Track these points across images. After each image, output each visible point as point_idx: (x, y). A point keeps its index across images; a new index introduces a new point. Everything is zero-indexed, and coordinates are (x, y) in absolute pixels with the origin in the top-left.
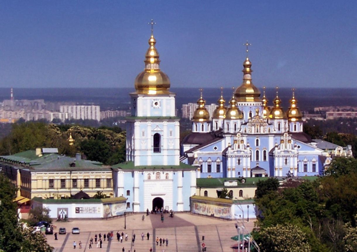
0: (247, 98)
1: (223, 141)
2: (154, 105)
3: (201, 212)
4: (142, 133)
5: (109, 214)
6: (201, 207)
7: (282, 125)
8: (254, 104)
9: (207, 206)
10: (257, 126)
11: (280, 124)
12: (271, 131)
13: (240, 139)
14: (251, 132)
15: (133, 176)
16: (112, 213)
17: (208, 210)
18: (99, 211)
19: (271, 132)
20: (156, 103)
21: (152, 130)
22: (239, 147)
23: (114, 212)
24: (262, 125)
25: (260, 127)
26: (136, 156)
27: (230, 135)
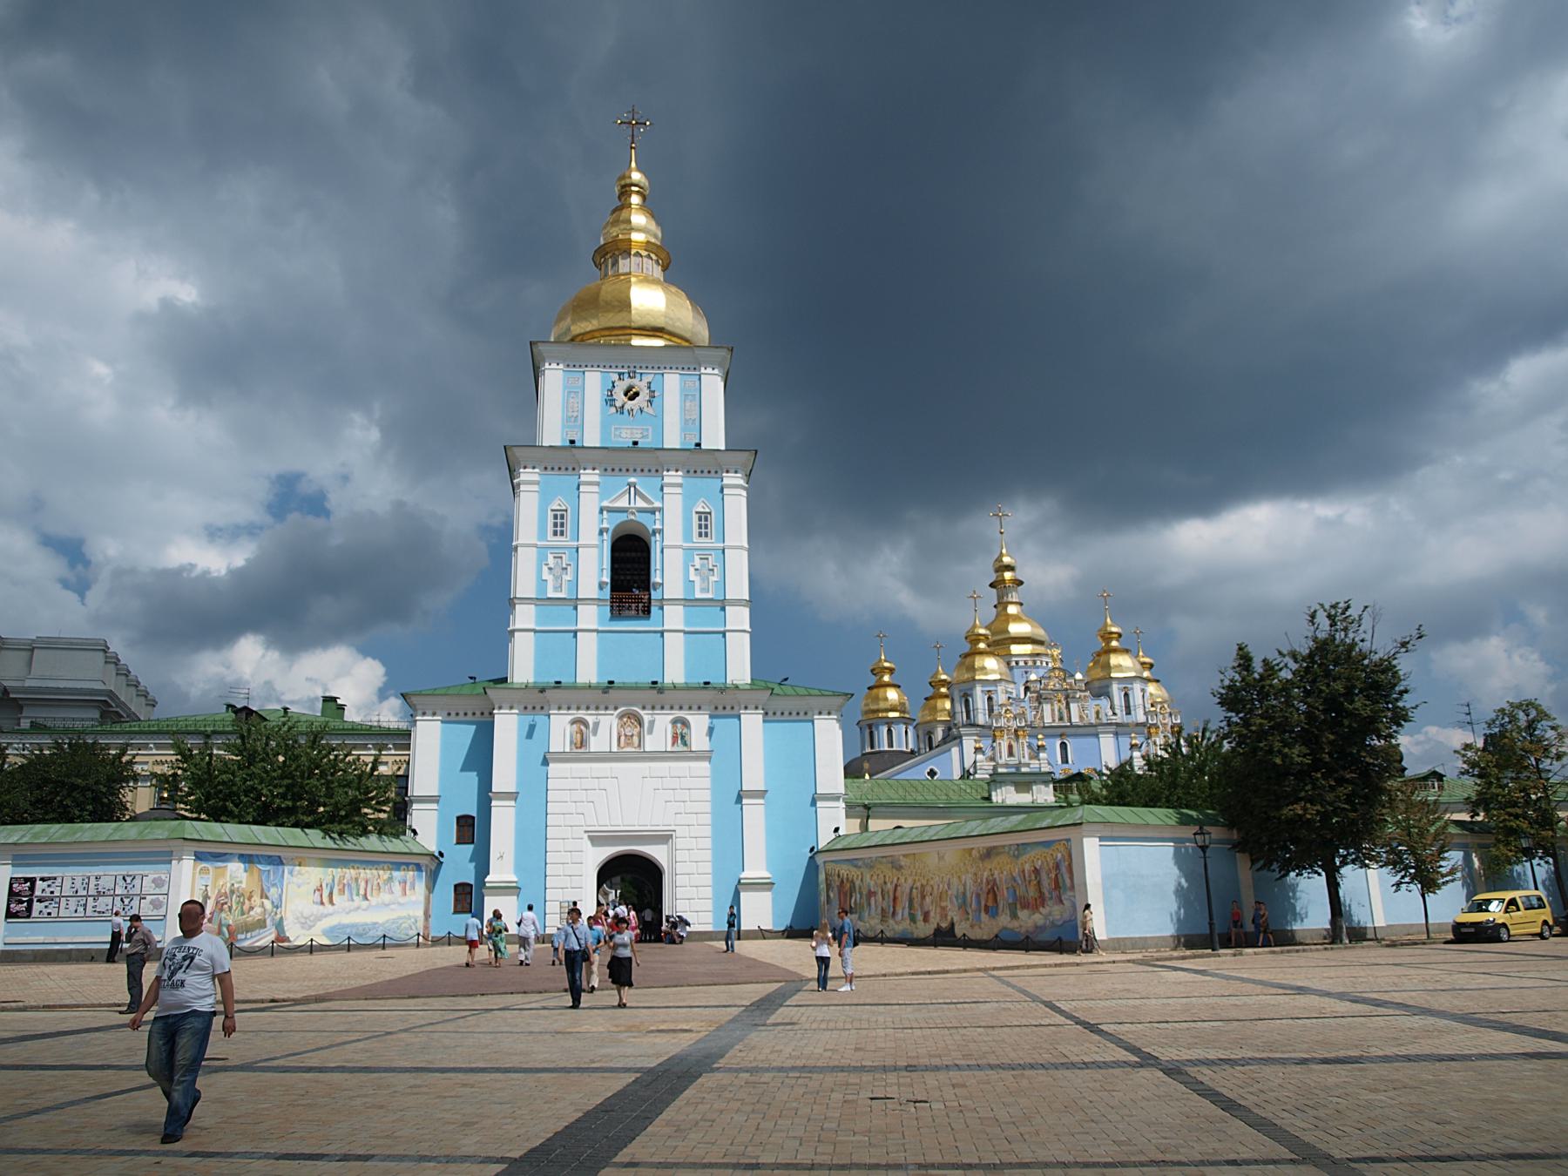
1: (955, 751)
3: (871, 923)
5: (261, 924)
6: (871, 894)
10: (1059, 701)
11: (1130, 692)
13: (1014, 724)
14: (1042, 717)
16: (279, 925)
17: (911, 906)
18: (156, 905)
19: (1105, 721)
20: (632, 395)
21: (605, 504)
22: (1011, 754)
23: (306, 924)
25: (1068, 704)
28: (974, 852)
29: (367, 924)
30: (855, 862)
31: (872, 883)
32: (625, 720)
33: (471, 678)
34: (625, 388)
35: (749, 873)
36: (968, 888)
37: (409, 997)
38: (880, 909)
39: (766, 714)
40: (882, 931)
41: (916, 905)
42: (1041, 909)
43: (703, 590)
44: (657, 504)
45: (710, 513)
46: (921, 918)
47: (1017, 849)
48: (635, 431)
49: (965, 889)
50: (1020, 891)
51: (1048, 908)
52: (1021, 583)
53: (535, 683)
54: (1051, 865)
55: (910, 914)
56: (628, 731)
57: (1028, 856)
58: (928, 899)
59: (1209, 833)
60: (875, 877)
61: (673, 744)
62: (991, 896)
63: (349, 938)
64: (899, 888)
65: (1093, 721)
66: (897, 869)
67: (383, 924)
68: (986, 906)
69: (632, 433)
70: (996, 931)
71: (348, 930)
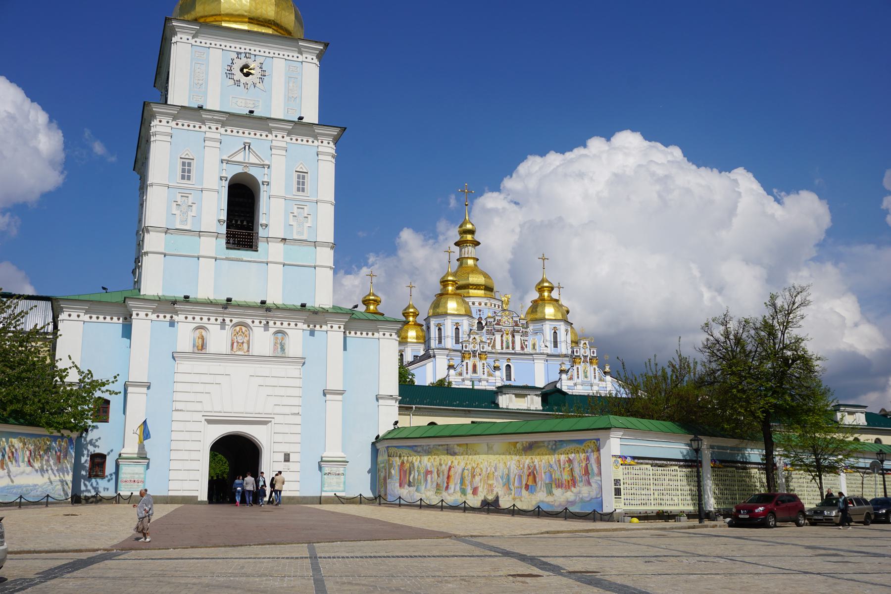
0: (471, 291)
2: (238, 75)
4: (179, 167)
6: (428, 472)
7: (562, 336)
8: (486, 304)
9: (459, 463)
10: (507, 334)
11: (557, 331)
12: (537, 347)
14: (494, 346)
15: (127, 332)
19: (538, 351)
20: (246, 71)
21: (225, 157)
22: (475, 370)
24: (518, 332)
25: (513, 336)
26: (146, 253)
27: (447, 352)
28: (518, 444)
29: (29, 486)
30: (416, 448)
31: (429, 465)
32: (238, 328)
33: (104, 288)
34: (241, 66)
35: (329, 454)
36: (512, 471)
37: (192, 547)
38: (435, 484)
39: (344, 332)
40: (442, 501)
41: (467, 482)
42: (573, 489)
43: (298, 233)
44: (267, 162)
45: (307, 173)
46: (471, 493)
47: (555, 445)
48: (248, 101)
49: (509, 470)
50: (556, 475)
51: (578, 488)
52: (478, 244)
53: (334, 307)
54: (582, 458)
55: (461, 489)
56: (240, 339)
57: (563, 450)
58: (477, 478)
59: (701, 440)
60: (433, 461)
61: (274, 351)
62: (531, 478)
63: (21, 497)
64: (452, 469)
65: (531, 351)
66: (451, 455)
67: (41, 487)
68: (526, 484)
69: (246, 103)
70: (534, 503)
71: (20, 491)
